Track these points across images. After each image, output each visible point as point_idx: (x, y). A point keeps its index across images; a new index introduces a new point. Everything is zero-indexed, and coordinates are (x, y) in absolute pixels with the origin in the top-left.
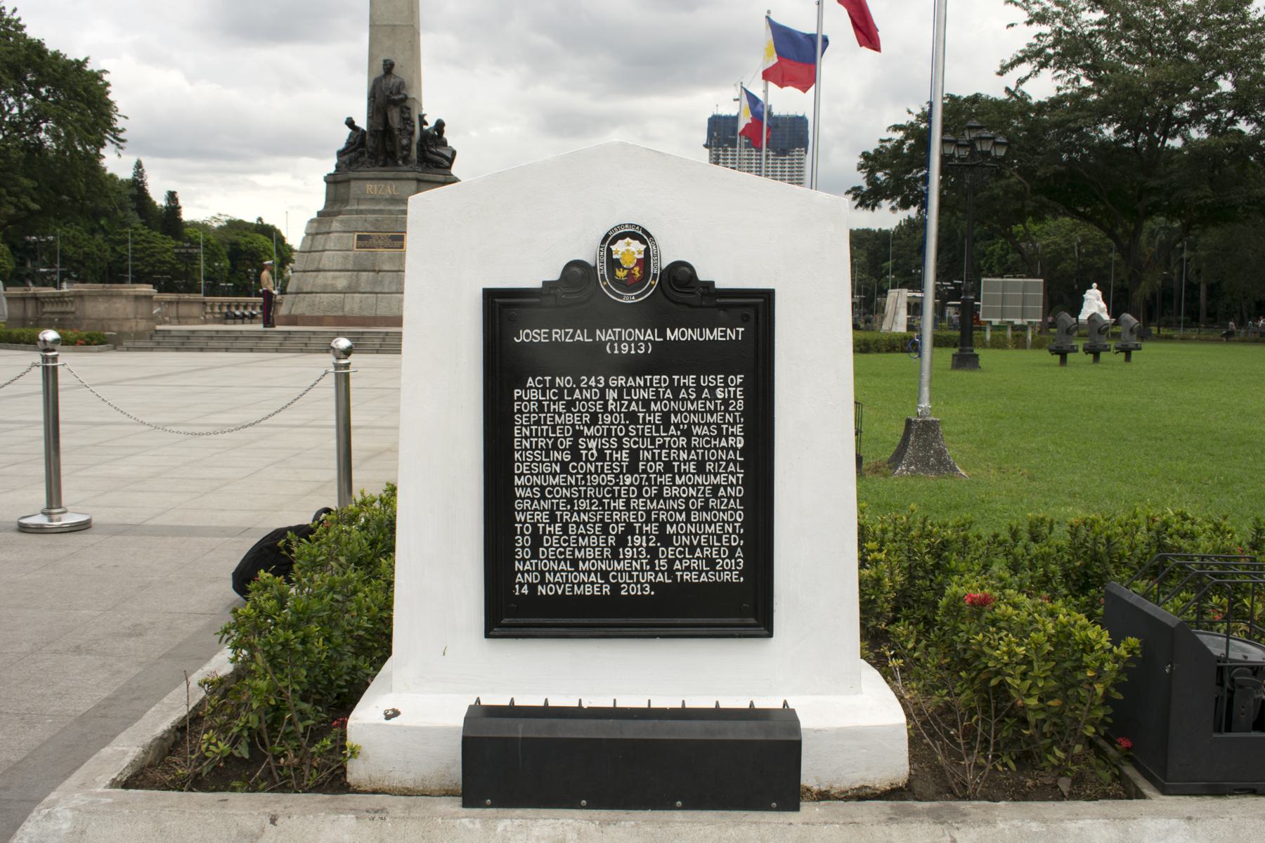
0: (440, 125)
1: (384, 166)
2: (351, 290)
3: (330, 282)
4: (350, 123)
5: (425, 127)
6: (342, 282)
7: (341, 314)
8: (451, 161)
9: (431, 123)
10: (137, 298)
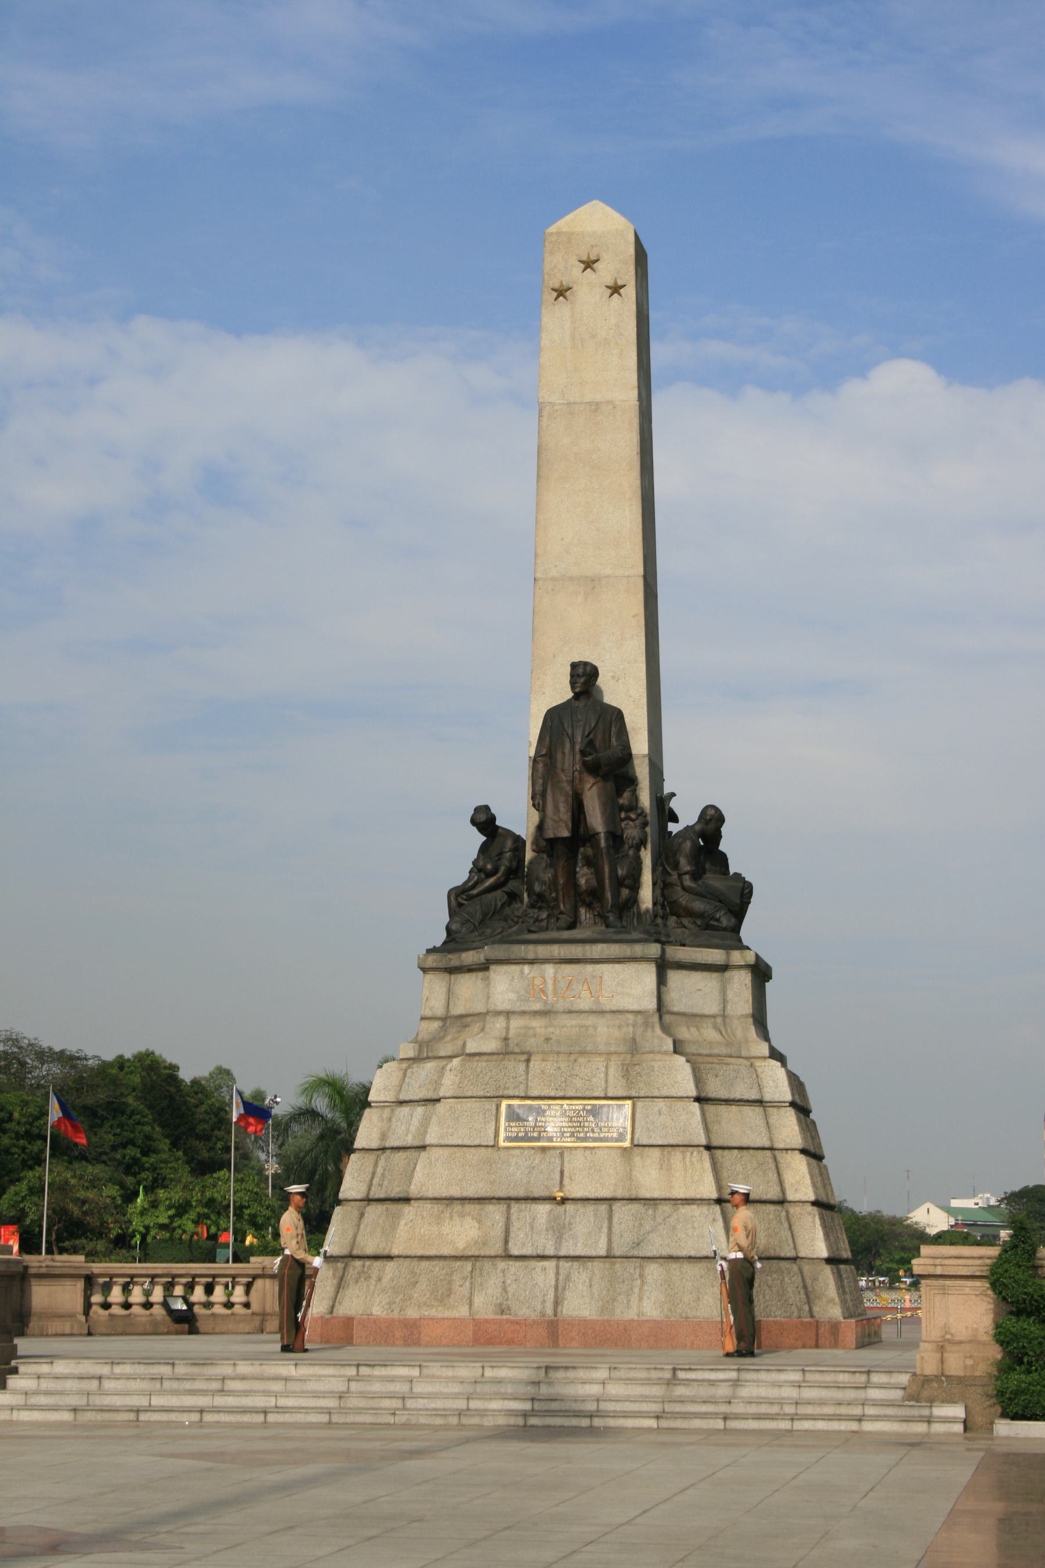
0: (712, 822)
1: (572, 926)
4: (485, 821)
7: (463, 1311)
8: (739, 912)
9: (687, 814)
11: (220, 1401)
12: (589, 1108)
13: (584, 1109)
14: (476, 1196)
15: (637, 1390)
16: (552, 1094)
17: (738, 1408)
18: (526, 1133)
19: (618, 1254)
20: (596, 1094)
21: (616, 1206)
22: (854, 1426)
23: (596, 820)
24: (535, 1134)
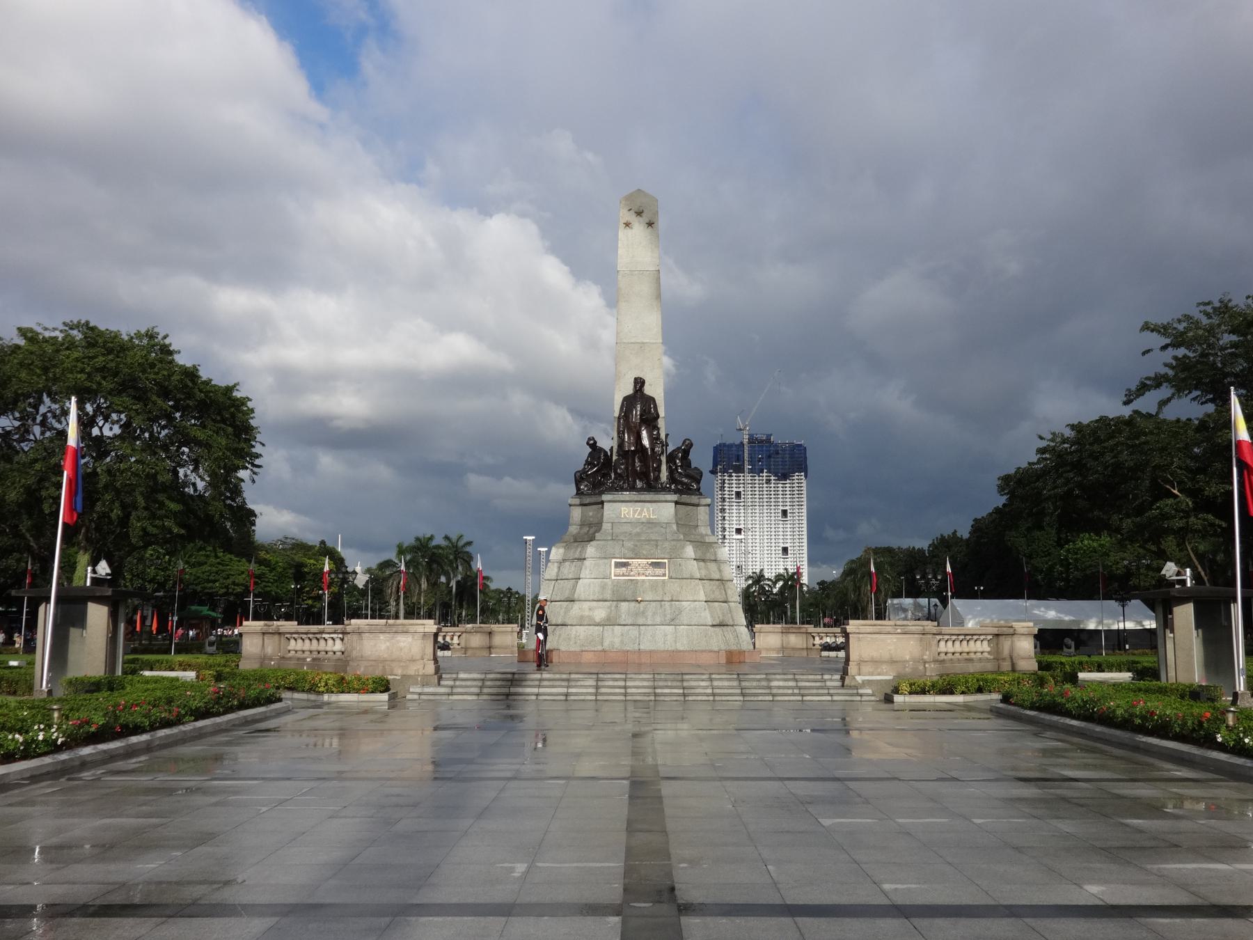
2: (610, 622)
3: (587, 613)
5: (670, 449)
6: (600, 613)
7: (600, 648)
10: (425, 635)
11: (542, 690)
15: (726, 683)
17: (774, 691)
22: (829, 698)
23: (646, 442)
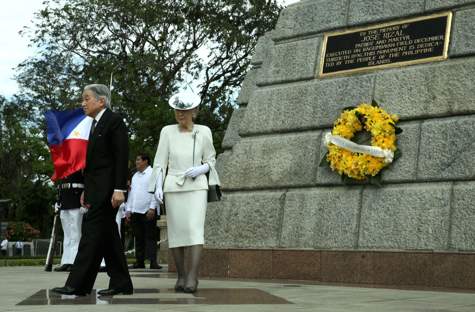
3: (257, 162)
7: (272, 243)
12: (406, 26)
13: (401, 28)
14: (295, 127)
16: (369, 18)
18: (343, 61)
19: (425, 177)
20: (413, 11)
21: (426, 123)
24: (352, 61)
